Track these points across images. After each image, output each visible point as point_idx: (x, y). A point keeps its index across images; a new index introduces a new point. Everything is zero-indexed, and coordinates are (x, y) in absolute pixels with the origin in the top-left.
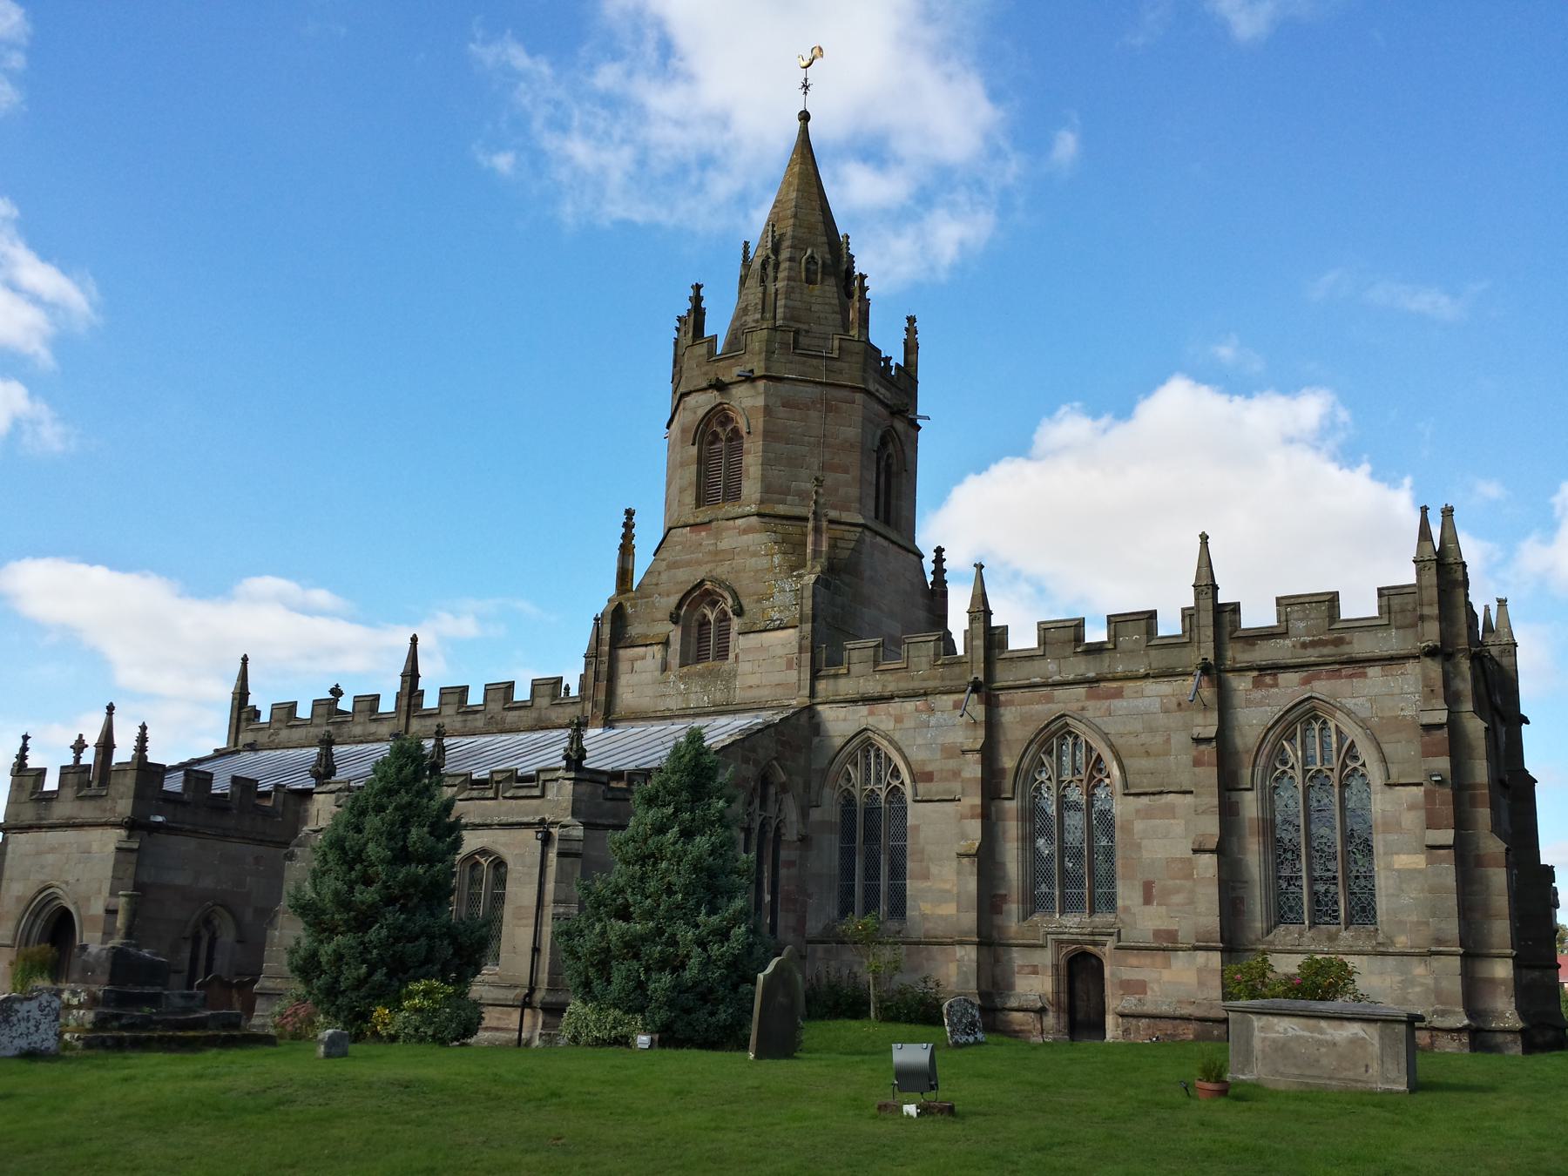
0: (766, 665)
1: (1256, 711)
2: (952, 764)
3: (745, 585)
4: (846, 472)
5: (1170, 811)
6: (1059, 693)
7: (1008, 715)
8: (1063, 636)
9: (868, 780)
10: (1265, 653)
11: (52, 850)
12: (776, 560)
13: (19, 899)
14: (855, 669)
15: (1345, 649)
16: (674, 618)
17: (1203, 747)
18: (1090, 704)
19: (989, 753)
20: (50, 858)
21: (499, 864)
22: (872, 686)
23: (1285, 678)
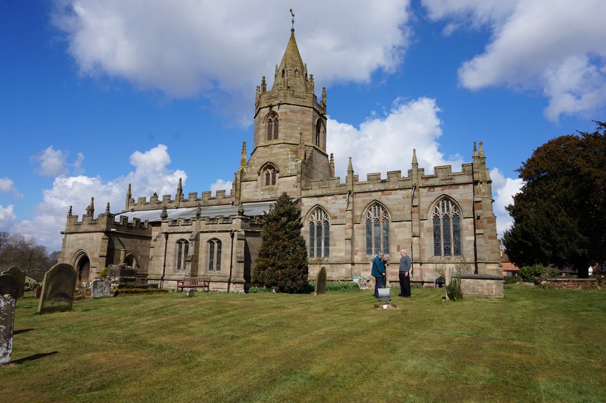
2: (343, 214)
4: (308, 131)
5: (405, 226)
6: (373, 194)
8: (374, 178)
9: (318, 219)
10: (431, 182)
11: (82, 239)
12: (289, 156)
13: (71, 253)
14: (313, 187)
15: (453, 181)
17: (415, 208)
18: (383, 197)
20: (81, 241)
21: (219, 242)
22: (319, 192)
23: (436, 189)
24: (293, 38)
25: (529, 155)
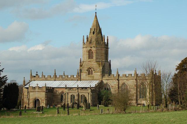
0: (97, 75)
1: (139, 82)
3: (95, 68)
7: (120, 82)
16: (87, 71)
19: (118, 85)
22: (108, 79)
24: (96, 16)
25: (180, 62)
